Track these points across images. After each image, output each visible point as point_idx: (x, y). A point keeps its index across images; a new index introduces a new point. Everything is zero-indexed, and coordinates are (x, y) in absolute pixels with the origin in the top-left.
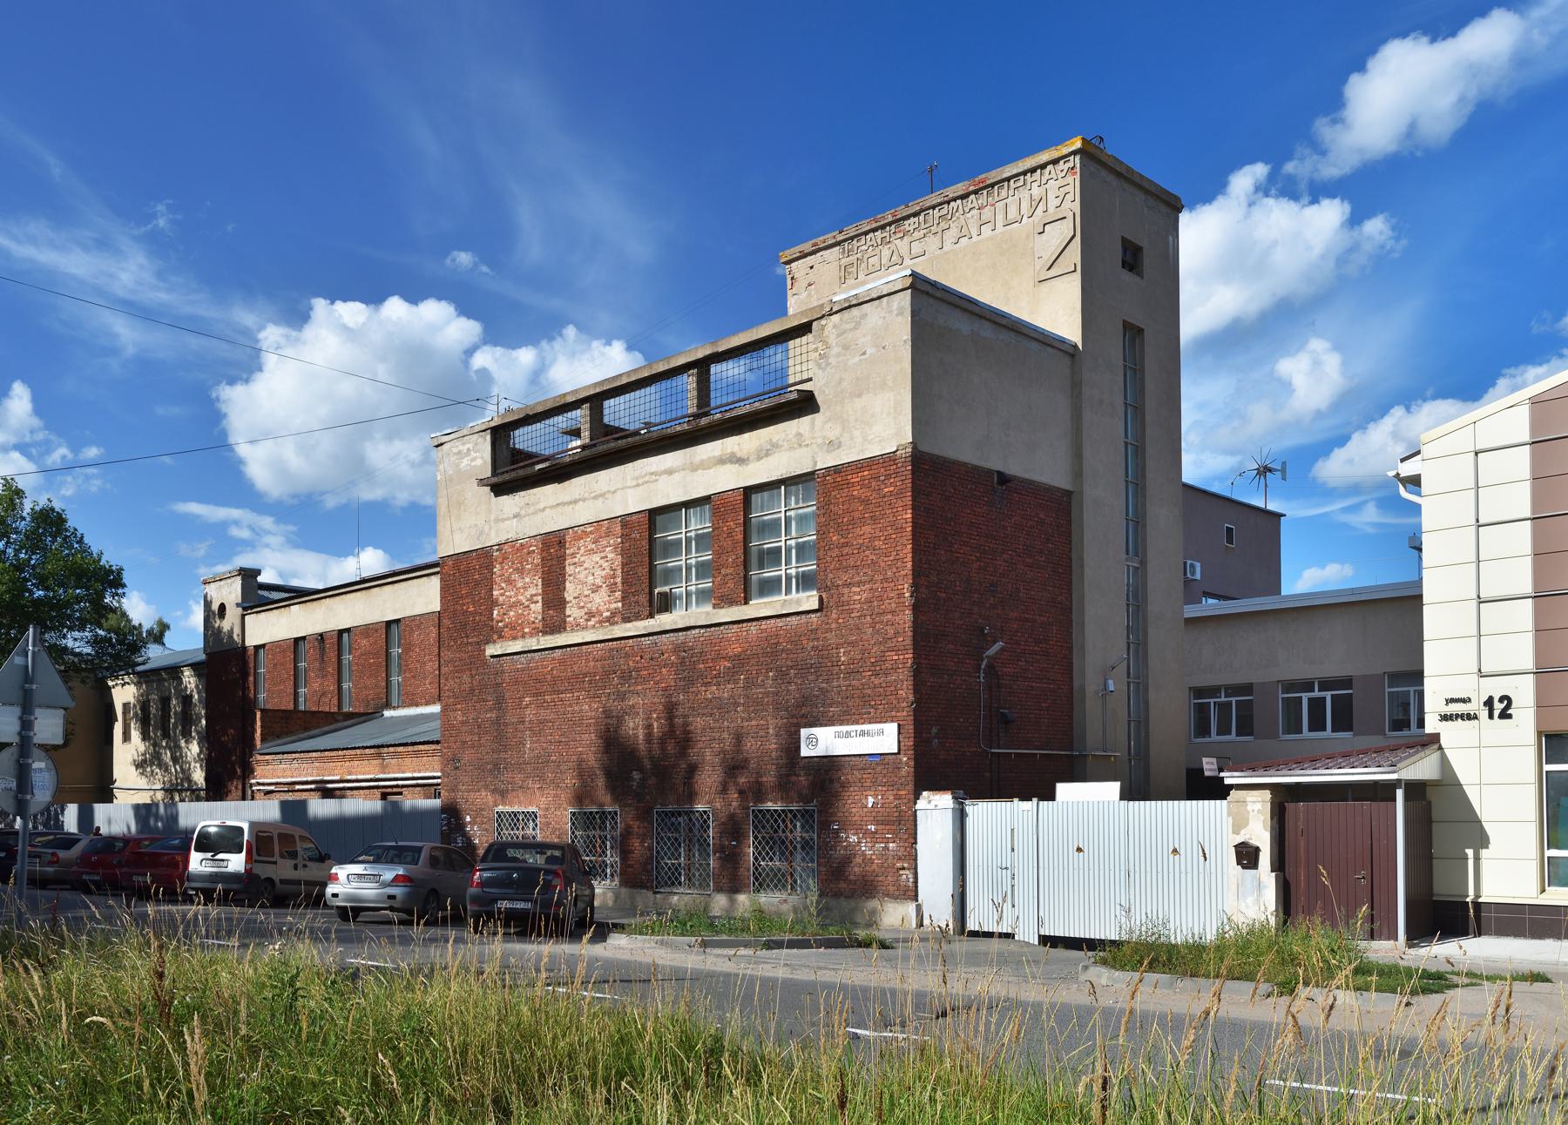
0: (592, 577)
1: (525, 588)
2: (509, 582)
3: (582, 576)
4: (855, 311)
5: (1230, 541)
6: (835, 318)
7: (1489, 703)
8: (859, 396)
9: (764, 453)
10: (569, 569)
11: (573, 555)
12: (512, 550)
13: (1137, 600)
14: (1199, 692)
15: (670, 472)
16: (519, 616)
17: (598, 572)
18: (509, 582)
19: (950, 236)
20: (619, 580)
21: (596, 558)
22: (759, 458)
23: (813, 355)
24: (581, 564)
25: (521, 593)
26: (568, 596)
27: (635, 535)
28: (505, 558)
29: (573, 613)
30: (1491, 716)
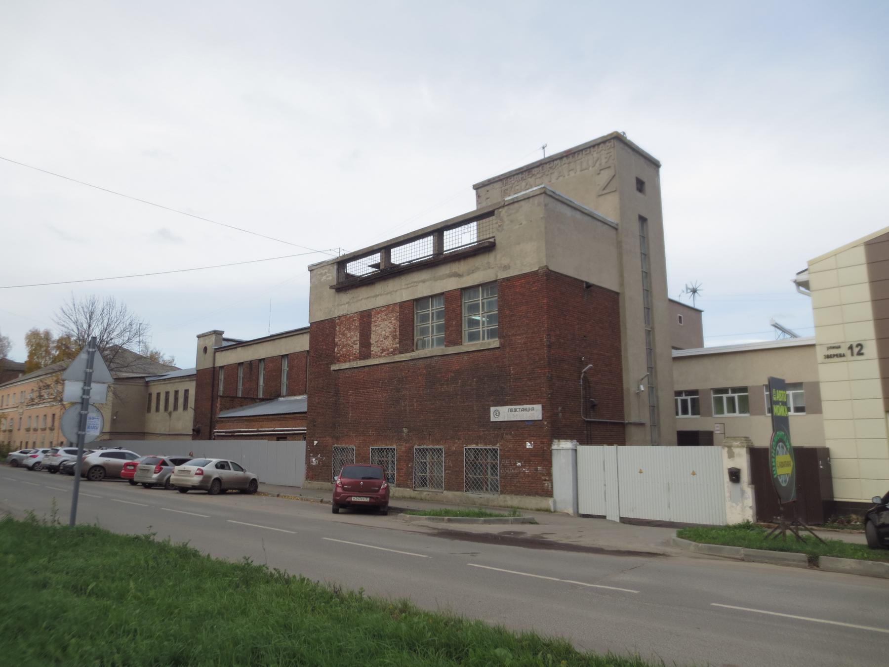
0: (384, 332)
1: (351, 337)
2: (343, 334)
3: (379, 332)
4: (516, 205)
5: (680, 322)
6: (506, 208)
7: (851, 348)
8: (519, 244)
9: (471, 272)
10: (373, 328)
11: (375, 322)
12: (345, 319)
13: (650, 350)
14: (678, 393)
15: (424, 281)
16: (348, 351)
17: (388, 330)
18: (343, 334)
19: (556, 174)
20: (398, 333)
21: (387, 323)
22: (469, 274)
23: (495, 226)
24: (379, 326)
25: (350, 340)
26: (372, 341)
27: (406, 311)
28: (341, 323)
29: (374, 349)
30: (852, 354)
